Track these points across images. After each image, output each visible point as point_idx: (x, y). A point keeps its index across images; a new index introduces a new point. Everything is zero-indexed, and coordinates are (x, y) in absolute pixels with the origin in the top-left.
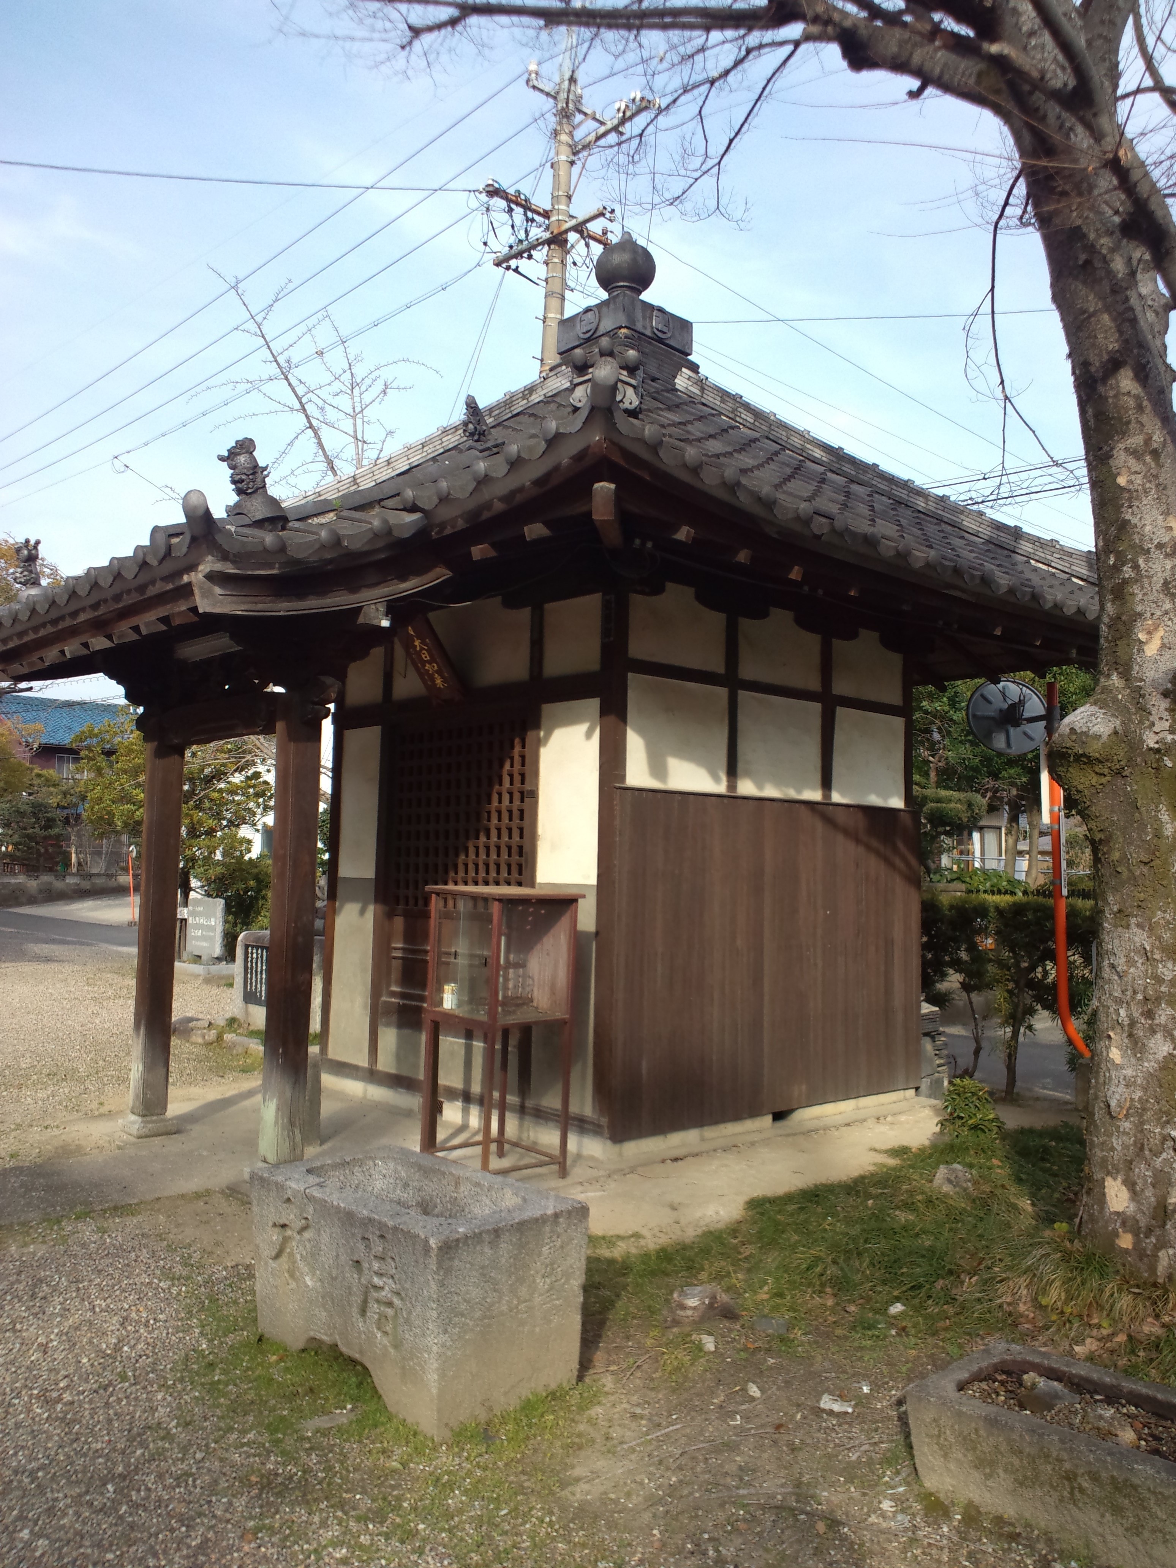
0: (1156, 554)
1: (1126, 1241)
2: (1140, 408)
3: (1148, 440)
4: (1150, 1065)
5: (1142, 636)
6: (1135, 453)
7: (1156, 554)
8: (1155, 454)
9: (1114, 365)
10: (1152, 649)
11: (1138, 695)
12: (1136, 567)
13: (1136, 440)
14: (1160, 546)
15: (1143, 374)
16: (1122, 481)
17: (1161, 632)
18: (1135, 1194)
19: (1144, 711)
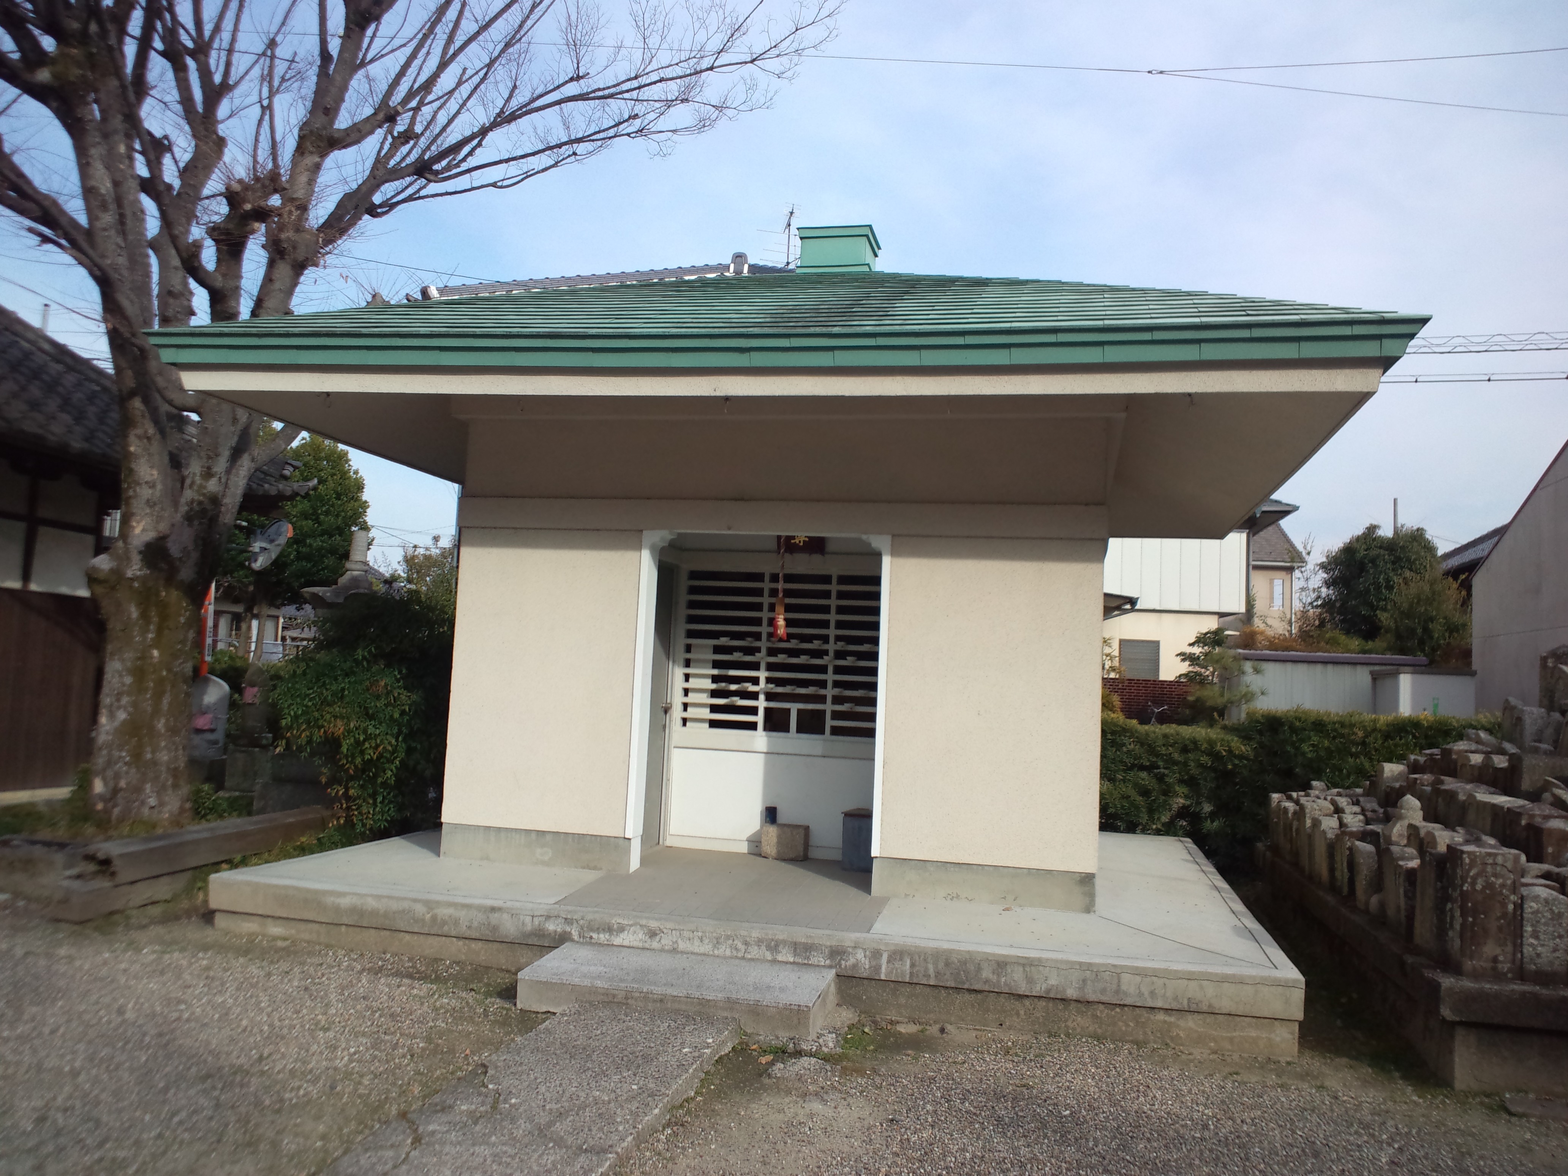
0: (144, 486)
1: (100, 806)
2: (143, 416)
3: (146, 432)
4: (116, 723)
5: (134, 524)
6: (139, 437)
7: (144, 486)
8: (149, 439)
9: (133, 394)
10: (138, 531)
11: (127, 551)
12: (135, 491)
13: (139, 431)
14: (146, 483)
15: (146, 401)
16: (132, 449)
17: (143, 523)
18: (106, 784)
19: (128, 559)
